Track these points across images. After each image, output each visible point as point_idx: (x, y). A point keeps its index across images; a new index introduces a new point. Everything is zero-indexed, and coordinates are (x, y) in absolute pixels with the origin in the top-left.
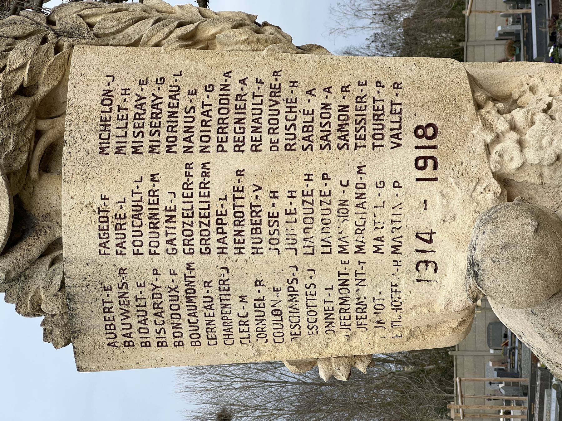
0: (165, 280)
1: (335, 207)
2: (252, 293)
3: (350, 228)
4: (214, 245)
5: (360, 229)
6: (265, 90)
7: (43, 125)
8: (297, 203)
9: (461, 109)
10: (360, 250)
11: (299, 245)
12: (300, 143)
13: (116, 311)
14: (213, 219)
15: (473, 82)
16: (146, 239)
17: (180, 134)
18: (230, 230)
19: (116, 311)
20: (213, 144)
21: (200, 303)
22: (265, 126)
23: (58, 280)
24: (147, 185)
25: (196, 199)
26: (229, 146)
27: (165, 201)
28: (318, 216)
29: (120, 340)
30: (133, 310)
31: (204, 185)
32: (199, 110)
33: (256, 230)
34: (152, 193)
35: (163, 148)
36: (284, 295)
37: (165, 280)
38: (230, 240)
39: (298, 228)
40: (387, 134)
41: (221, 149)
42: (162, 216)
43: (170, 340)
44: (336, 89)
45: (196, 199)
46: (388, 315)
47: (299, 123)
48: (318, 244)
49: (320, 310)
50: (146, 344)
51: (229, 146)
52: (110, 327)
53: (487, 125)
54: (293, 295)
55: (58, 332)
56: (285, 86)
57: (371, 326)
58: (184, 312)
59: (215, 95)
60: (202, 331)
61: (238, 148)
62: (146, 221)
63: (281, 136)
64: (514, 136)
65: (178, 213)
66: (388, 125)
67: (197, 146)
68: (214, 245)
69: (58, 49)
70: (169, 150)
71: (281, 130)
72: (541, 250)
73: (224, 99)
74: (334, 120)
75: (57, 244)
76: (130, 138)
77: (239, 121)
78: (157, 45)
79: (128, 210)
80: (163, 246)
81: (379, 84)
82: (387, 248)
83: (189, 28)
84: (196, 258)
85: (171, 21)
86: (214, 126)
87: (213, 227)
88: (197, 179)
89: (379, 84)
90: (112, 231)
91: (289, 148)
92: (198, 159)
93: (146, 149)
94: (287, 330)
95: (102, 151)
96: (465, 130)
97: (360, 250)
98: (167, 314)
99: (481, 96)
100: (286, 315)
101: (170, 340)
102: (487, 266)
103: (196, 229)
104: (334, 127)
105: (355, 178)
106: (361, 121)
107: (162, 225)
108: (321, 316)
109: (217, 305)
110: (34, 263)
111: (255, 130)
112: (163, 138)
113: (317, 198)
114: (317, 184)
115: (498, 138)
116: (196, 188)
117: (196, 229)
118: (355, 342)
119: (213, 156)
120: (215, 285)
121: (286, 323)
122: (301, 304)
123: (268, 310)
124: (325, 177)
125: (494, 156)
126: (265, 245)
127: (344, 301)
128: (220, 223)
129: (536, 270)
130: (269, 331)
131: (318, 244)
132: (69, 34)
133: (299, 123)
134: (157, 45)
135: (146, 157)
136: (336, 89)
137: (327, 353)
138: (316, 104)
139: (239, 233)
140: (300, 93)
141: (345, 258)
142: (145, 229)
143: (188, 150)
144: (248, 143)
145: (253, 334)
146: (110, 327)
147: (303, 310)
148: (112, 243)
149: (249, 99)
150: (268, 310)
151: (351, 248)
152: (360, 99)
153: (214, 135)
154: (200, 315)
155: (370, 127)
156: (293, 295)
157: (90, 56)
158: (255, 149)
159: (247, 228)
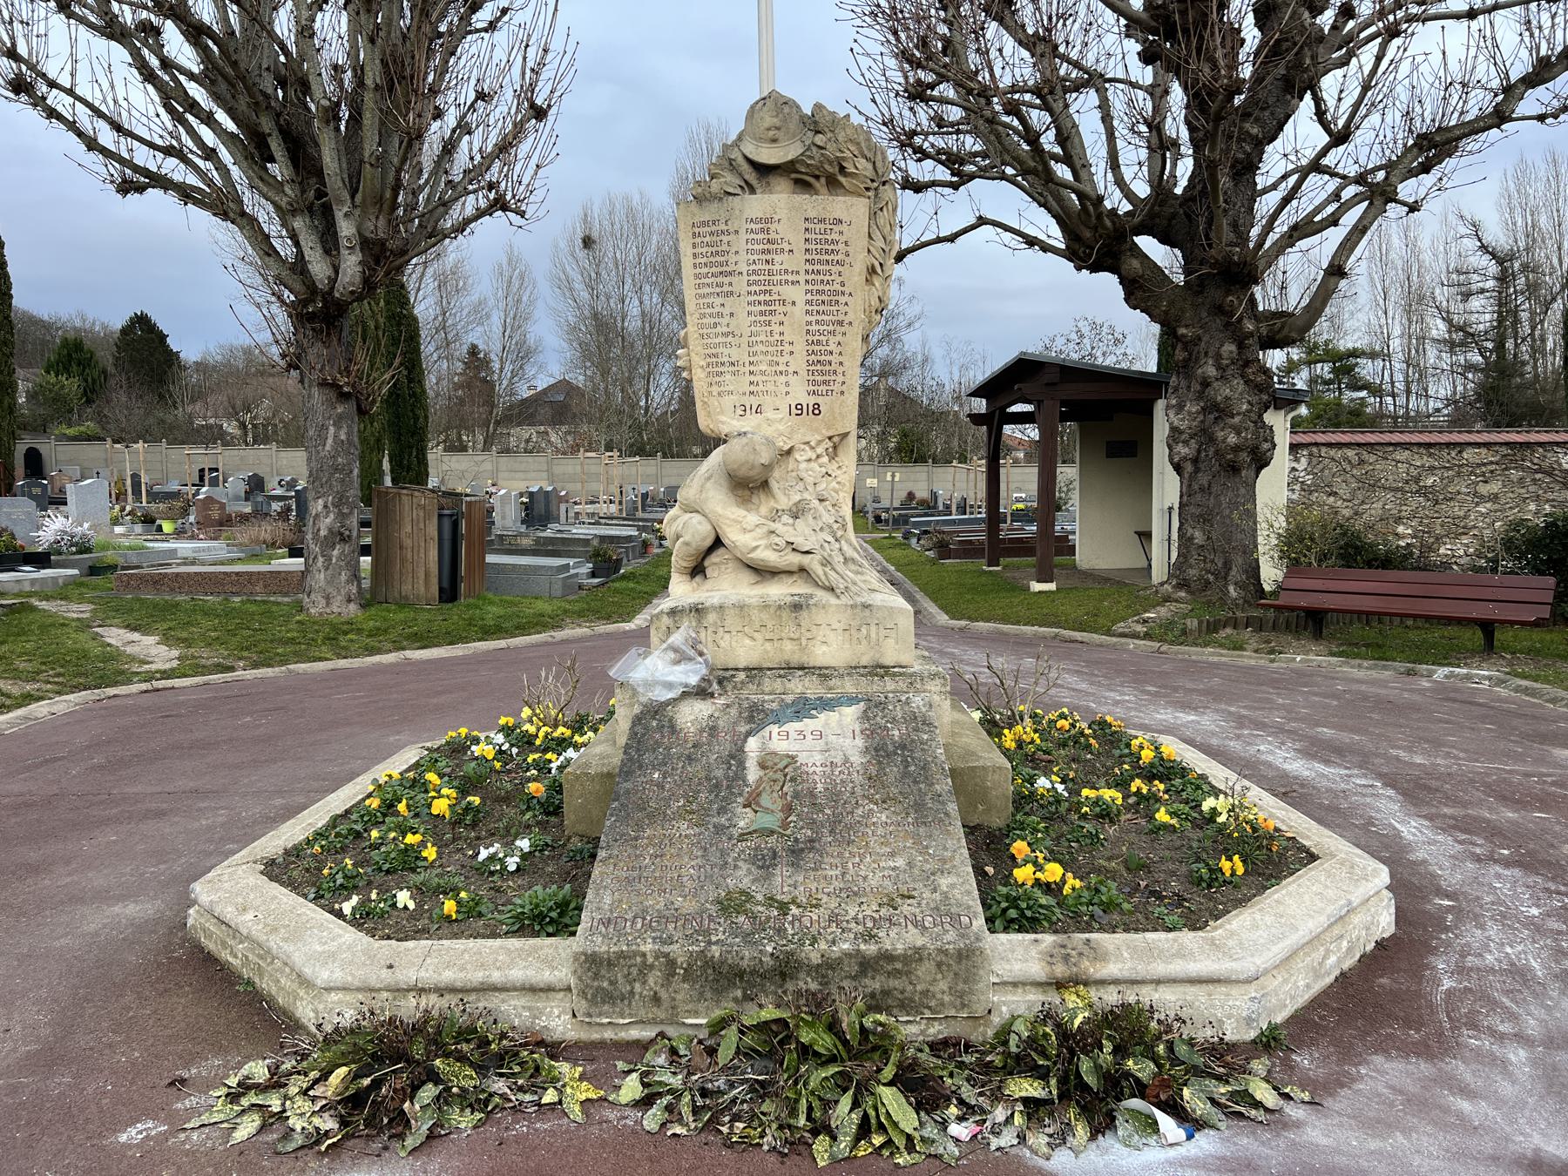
0: (732, 258)
1: (775, 359)
2: (726, 311)
3: (763, 367)
4: (753, 288)
5: (763, 373)
6: (841, 317)
7: (823, 180)
8: (777, 337)
9: (828, 429)
10: (751, 373)
11: (753, 338)
12: (810, 338)
13: (714, 228)
14: (768, 288)
15: (845, 435)
16: (756, 247)
17: (816, 267)
18: (762, 298)
19: (714, 228)
20: (810, 287)
21: (720, 279)
22: (820, 318)
23: (731, 190)
24: (787, 247)
25: (779, 277)
26: (809, 296)
27: (778, 258)
28: (770, 349)
29: (697, 230)
30: (714, 238)
31: (787, 282)
32: (830, 278)
33: (762, 313)
34: (782, 251)
35: (808, 257)
36: (725, 329)
37: (732, 258)
38: (756, 297)
39: (763, 338)
40: (816, 388)
41: (807, 292)
42: (769, 257)
43: (698, 261)
44: (841, 359)
45: (779, 277)
46: (715, 389)
47: (822, 338)
48: (754, 349)
49: (718, 350)
50: (694, 246)
51: (809, 296)
52: (704, 224)
53: (819, 442)
54: (726, 335)
55: (700, 190)
56: (843, 329)
57: (709, 380)
58: (714, 270)
59: (838, 287)
60: (703, 281)
61: (808, 302)
62: (766, 247)
63: (814, 327)
64: (814, 457)
65: (770, 267)
66: (820, 388)
67: (810, 277)
68: (753, 288)
69: (868, 189)
70: (808, 261)
71: (817, 327)
72: (753, 467)
73: (836, 293)
74: (823, 358)
75: (752, 190)
76: (814, 236)
77: (823, 302)
78: (869, 251)
79: (772, 236)
80: (752, 258)
81: (844, 383)
82: (752, 388)
83: (879, 270)
84: (746, 278)
85: (884, 259)
86: (821, 287)
87: (763, 288)
88: (790, 278)
89: (844, 383)
90: (760, 226)
91: (808, 332)
92: (802, 278)
93: (808, 246)
94: (705, 331)
95: (807, 219)
96: (817, 430)
97: (751, 373)
98: (712, 259)
99: (836, 439)
100: (714, 330)
101: (698, 261)
102: (744, 440)
103: (762, 278)
104: (819, 358)
105: (791, 370)
106: (822, 373)
107: (764, 257)
108: (714, 351)
109: (718, 290)
110: (741, 175)
111: (818, 312)
112: (814, 257)
113: (780, 348)
114: (787, 348)
115: (812, 448)
116: (784, 277)
117: (762, 278)
118: (699, 370)
119: (804, 287)
120: (730, 289)
121: (709, 331)
122: (720, 339)
123: (717, 320)
124: (792, 353)
125: (802, 446)
126: (753, 318)
127: (723, 364)
128: (765, 292)
129: (742, 465)
130: (704, 321)
131: (754, 349)
132: (876, 196)
133: (822, 338)
134: (869, 251)
135: (803, 246)
136: (841, 359)
137: (692, 354)
138: (832, 347)
139: (760, 303)
140: (839, 338)
141: (747, 364)
142: (761, 246)
143: (807, 272)
144: (810, 308)
145: (702, 311)
146: (704, 224)
147: (717, 341)
148: (753, 226)
149: (834, 308)
150: (717, 320)
151: (752, 368)
152: (835, 372)
153: (815, 287)
154: (712, 279)
155: (819, 378)
156: (726, 335)
157: (863, 210)
158: (807, 312)
159: (763, 308)
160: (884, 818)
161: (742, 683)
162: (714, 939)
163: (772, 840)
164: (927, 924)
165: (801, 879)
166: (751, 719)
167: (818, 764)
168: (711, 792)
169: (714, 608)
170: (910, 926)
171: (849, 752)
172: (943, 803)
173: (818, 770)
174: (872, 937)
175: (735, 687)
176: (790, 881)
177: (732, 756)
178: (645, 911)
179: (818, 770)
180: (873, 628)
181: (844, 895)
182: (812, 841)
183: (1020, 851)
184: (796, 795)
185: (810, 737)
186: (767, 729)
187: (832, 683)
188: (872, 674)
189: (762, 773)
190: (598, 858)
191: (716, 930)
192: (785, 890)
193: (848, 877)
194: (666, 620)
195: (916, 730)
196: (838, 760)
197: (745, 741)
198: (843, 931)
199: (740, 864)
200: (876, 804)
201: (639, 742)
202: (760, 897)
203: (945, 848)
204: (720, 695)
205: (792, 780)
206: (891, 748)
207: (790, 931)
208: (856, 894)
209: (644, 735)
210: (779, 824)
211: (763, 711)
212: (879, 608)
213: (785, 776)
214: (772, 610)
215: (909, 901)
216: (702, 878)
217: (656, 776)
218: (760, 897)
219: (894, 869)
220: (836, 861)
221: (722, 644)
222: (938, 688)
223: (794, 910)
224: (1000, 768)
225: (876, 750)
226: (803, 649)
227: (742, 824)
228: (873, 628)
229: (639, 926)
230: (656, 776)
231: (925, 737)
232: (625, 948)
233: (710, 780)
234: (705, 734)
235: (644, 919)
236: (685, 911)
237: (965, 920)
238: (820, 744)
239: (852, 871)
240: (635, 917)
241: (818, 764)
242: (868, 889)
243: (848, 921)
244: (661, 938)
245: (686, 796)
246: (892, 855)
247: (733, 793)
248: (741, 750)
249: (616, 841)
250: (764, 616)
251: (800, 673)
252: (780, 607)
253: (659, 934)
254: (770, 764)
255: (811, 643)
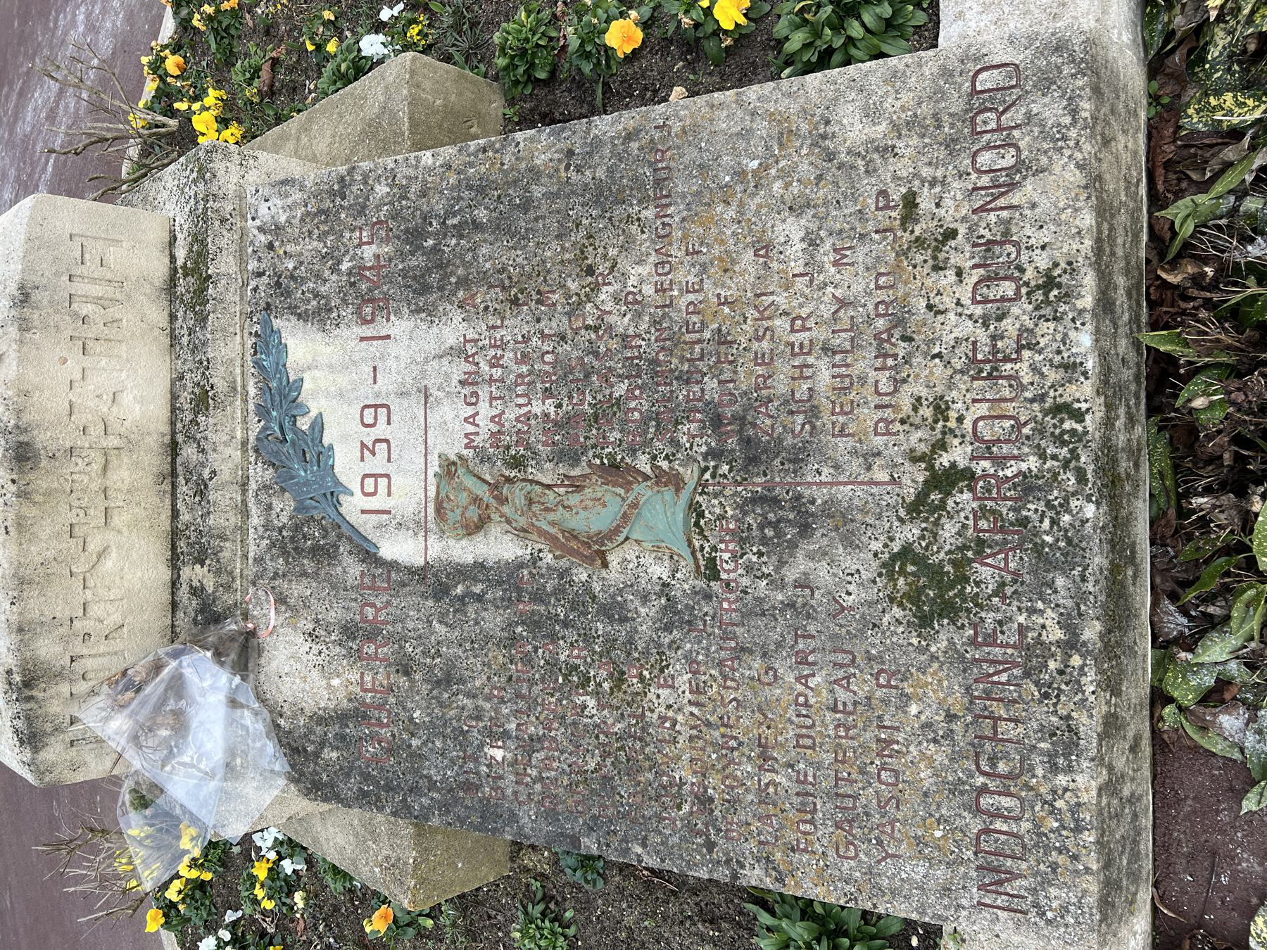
160: (644, 270)
161: (218, 572)
162: (1056, 634)
163: (714, 511)
164: (1009, 161)
165: (843, 444)
166: (324, 553)
167: (470, 411)
168: (554, 638)
169: (22, 646)
170: (1016, 198)
171: (432, 347)
172: (597, 144)
173: (485, 410)
174: (1049, 282)
175: (228, 588)
176: (855, 465)
177: (441, 591)
178: (955, 789)
179: (485, 410)
180: (80, 288)
181: (902, 349)
182: (717, 422)
183: (628, 39)
184: (568, 455)
185: (381, 430)
186: (355, 518)
187: (220, 385)
188: (200, 295)
189: (495, 530)
190: (769, 883)
191: (1022, 630)
192: (883, 476)
193: (842, 340)
194: (53, 752)
195: (361, 210)
196: (458, 369)
197: (393, 565)
198: (1030, 347)
199: (791, 574)
200: (596, 288)
201: (389, 788)
202: (910, 533)
203: (746, 134)
204: (246, 616)
205: (517, 463)
206: (418, 261)
207: (1033, 463)
208: (900, 322)
209: (366, 777)
210: (668, 493)
211: (297, 528)
212: (28, 268)
213: (509, 480)
214: (30, 511)
215: (925, 203)
216: (840, 657)
217: (498, 754)
218: (910, 533)
219: (812, 241)
220: (784, 370)
221: (116, 618)
222: (234, 168)
223: (958, 455)
224: (413, 73)
225: (425, 289)
226: (130, 444)
227: (660, 571)
228: (80, 288)
229: (1006, 802)
230: (498, 754)
231: (382, 190)
232: (1089, 837)
233: (513, 640)
234: (370, 649)
235: (984, 790)
236: (957, 700)
237: (987, 80)
238: (407, 410)
239: (821, 334)
240: (977, 811)
241: (470, 411)
242: (882, 295)
243: (994, 338)
244: (1051, 755)
245: (566, 691)
246: (764, 248)
247: (559, 592)
248: (420, 574)
249: (710, 845)
250: (45, 530)
251: (189, 452)
252: (23, 495)
253: (1036, 759)
254: (473, 513)
255: (115, 426)
